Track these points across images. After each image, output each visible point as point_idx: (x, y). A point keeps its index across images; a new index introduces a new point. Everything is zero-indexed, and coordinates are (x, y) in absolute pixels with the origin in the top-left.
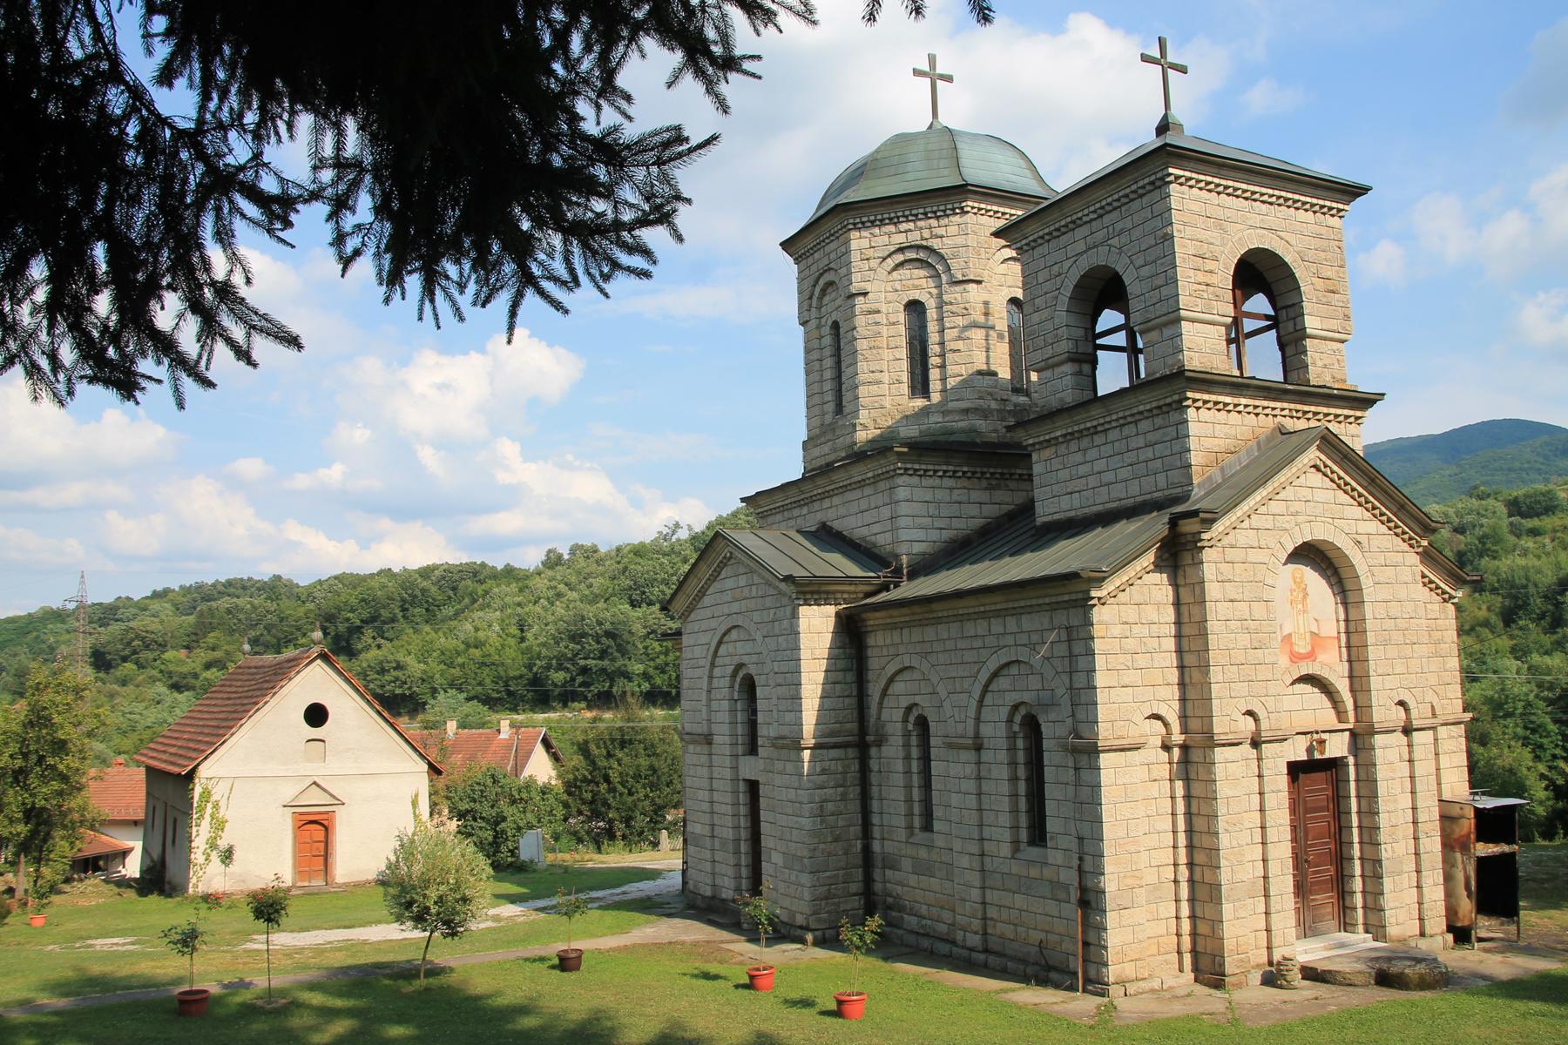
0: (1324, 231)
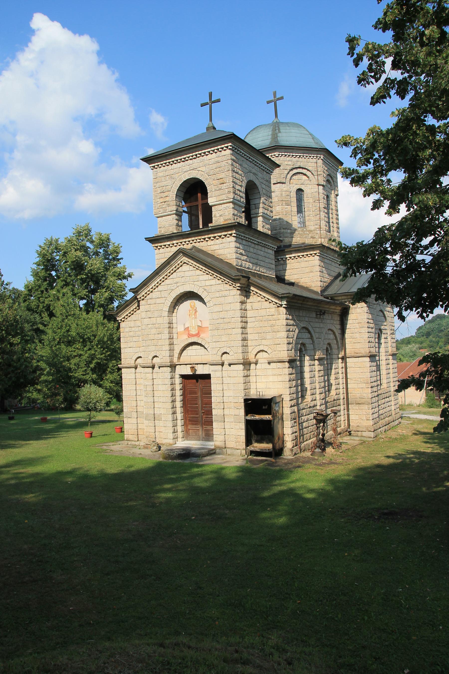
0: (220, 159)
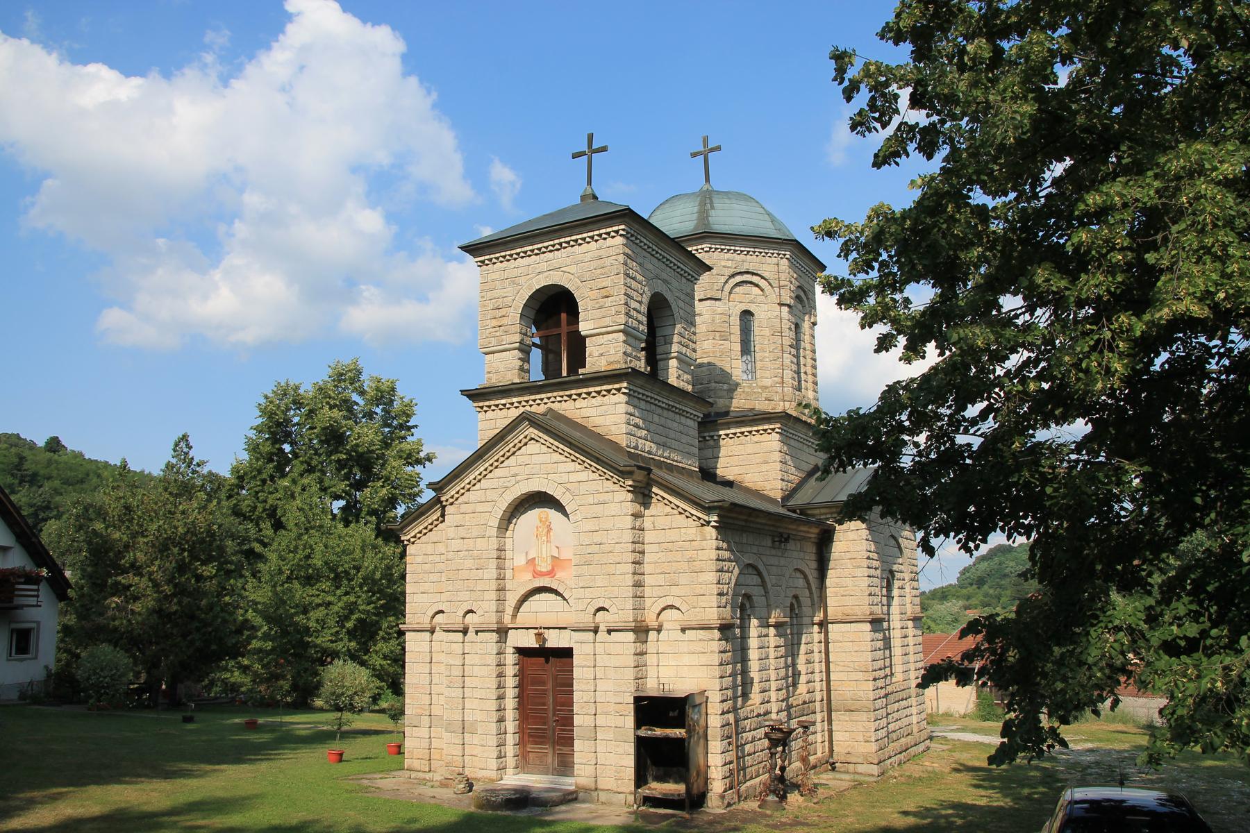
0: (602, 253)
